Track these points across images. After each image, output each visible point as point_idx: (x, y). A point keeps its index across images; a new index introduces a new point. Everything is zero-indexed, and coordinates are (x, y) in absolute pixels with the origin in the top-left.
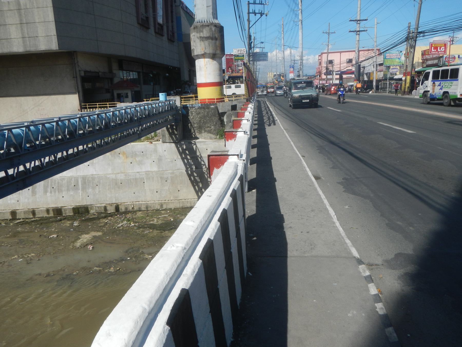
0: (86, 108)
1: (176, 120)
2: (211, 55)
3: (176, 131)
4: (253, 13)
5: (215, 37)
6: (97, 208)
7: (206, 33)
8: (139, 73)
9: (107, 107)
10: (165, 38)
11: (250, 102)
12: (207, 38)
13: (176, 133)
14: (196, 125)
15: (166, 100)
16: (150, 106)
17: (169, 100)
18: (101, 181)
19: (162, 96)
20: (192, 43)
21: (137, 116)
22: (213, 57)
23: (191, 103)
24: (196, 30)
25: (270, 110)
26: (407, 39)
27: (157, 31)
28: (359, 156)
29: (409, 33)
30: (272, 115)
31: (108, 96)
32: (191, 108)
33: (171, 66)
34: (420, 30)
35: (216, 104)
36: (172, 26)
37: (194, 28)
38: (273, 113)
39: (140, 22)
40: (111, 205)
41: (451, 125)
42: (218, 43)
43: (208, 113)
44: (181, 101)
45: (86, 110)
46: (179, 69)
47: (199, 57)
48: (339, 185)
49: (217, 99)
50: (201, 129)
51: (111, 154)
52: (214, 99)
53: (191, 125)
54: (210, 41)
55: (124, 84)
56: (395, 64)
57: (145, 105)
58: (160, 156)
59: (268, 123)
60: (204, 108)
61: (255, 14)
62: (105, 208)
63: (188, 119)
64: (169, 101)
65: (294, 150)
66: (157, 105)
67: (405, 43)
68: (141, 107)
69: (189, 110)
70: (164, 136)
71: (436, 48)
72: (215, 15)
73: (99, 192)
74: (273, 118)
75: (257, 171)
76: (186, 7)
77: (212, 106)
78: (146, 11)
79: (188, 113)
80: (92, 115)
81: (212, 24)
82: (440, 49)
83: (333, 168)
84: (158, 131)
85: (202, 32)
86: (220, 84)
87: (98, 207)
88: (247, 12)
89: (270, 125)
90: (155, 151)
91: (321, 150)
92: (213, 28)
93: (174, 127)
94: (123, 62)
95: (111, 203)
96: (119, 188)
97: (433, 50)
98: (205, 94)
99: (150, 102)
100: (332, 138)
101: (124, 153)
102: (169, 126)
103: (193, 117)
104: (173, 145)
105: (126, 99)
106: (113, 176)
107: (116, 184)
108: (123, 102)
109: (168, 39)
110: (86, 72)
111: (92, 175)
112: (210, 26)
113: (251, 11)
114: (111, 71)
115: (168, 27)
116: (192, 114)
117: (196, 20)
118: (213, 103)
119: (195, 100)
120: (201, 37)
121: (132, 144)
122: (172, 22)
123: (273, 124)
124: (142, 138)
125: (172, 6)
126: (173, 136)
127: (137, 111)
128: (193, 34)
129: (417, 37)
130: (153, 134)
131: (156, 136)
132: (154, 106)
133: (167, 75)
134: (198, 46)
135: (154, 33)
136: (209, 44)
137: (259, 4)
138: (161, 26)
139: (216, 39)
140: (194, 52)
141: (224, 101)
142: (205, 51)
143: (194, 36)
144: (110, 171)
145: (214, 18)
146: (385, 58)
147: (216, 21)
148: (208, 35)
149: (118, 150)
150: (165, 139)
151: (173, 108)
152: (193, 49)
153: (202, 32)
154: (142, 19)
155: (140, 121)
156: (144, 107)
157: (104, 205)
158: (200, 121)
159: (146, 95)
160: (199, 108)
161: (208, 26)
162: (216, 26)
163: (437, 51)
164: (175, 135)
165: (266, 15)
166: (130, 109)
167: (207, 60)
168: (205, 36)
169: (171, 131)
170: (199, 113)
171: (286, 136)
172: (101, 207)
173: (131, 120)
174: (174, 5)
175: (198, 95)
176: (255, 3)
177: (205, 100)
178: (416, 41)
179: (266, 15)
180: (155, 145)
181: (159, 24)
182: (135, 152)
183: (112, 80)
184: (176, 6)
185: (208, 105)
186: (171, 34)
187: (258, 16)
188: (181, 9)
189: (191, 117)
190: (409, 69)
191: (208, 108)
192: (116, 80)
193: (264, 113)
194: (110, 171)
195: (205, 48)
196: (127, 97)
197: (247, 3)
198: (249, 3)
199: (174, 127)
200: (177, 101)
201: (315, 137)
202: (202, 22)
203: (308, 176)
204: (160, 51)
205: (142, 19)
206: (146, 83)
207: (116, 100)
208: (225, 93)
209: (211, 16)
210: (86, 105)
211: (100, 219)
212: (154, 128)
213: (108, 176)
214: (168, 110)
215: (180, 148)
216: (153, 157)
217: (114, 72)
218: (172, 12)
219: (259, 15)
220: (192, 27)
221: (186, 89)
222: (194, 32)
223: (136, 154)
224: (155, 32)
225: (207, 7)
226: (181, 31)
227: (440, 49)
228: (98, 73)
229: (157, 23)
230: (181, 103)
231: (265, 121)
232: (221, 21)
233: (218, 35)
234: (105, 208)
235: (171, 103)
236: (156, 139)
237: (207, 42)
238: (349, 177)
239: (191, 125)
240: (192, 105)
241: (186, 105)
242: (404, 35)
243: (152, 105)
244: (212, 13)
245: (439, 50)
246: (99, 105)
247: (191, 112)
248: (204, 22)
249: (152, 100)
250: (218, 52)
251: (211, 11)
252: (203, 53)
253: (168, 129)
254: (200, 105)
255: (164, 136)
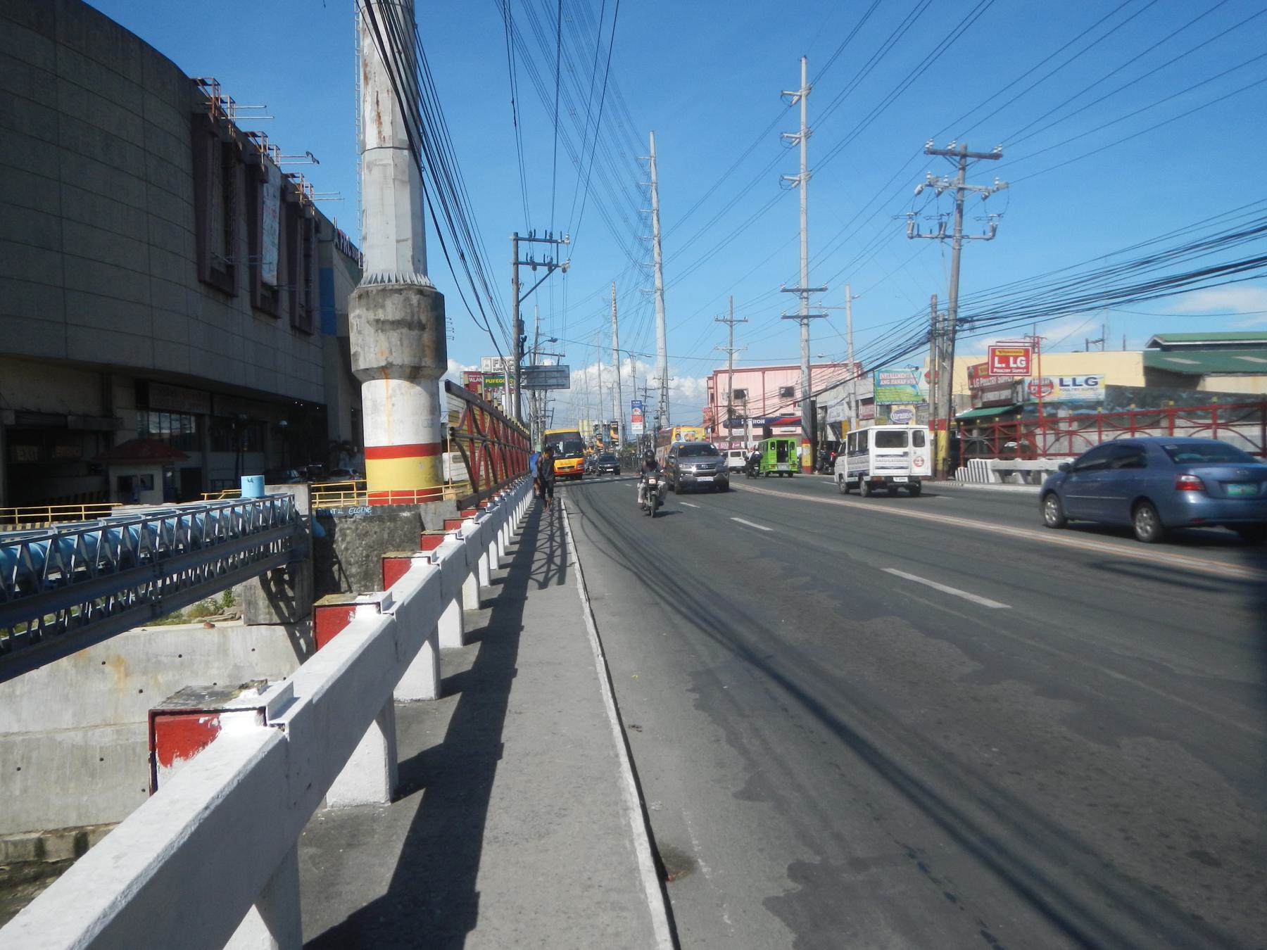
0: (12, 521)
1: (292, 556)
2: (408, 371)
3: (292, 588)
4: (527, 263)
5: (420, 322)
6: (11, 849)
7: (392, 309)
8: (199, 417)
9: (79, 518)
10: (284, 323)
11: (479, 507)
12: (396, 324)
13: (290, 593)
14: (354, 570)
15: (262, 497)
16: (203, 516)
17: (272, 496)
18: (34, 754)
19: (249, 486)
20: (353, 337)
21: (149, 548)
22: (413, 374)
23: (342, 505)
24: (363, 301)
25: (562, 528)
26: (932, 336)
27: (259, 303)
28: (843, 716)
29: (935, 320)
30: (563, 545)
31: (94, 483)
32: (340, 518)
33: (300, 401)
34: (961, 315)
35: (416, 507)
36: (307, 294)
37: (360, 297)
38: (569, 539)
39: (207, 277)
40: (60, 833)
41: (1107, 575)
42: (427, 337)
43: (391, 533)
44: (311, 498)
45: (10, 527)
46: (324, 408)
47: (373, 374)
48: (777, 923)
49: (420, 492)
50: (371, 581)
51: (75, 666)
52: (411, 493)
53: (340, 568)
54: (405, 331)
55: (148, 449)
56: (905, 399)
57: (209, 509)
58: (236, 667)
59: (541, 577)
60: (381, 519)
61: (534, 266)
62: (40, 846)
63: (333, 551)
64: (272, 498)
65: (601, 701)
66: (227, 512)
67: (928, 346)
68: (131, 528)
69: (335, 525)
70: (251, 603)
71: (1005, 360)
72: (420, 263)
73: (25, 790)
74: (565, 554)
75: (408, 843)
76: (351, 246)
77: (406, 514)
78: (228, 250)
79: (331, 534)
80: (34, 541)
81: (411, 286)
82: (1015, 362)
83: (749, 798)
84: (237, 589)
85: (383, 307)
86: (433, 450)
87: (15, 844)
88: (512, 259)
89: (543, 585)
90: (223, 650)
91: (705, 688)
92: (415, 299)
93: (286, 577)
94: (148, 388)
95: (61, 826)
96: (93, 775)
97: (997, 365)
98: (385, 477)
99: (204, 503)
100: (749, 636)
101: (119, 661)
102: (269, 574)
103: (347, 545)
104: (281, 631)
105: (148, 492)
106: (77, 737)
107: (85, 762)
108: (136, 501)
109: (293, 327)
110: (20, 413)
111: (6, 735)
112: (404, 293)
113: (522, 258)
114: (107, 412)
115: (292, 295)
116: (344, 535)
117: (366, 275)
118: (409, 505)
119: (359, 495)
120: (378, 321)
121: (136, 631)
122: (307, 281)
123: (555, 579)
124: (186, 610)
125: (307, 240)
126: (282, 604)
127: (154, 532)
128: (357, 312)
129: (955, 332)
130: (219, 597)
131: (229, 602)
132: (216, 514)
133: (285, 423)
134: (369, 344)
135: (248, 310)
136: (401, 340)
137: (545, 241)
138: (273, 292)
139: (422, 327)
140: (357, 360)
141: (440, 498)
142: (390, 360)
143: (359, 316)
144: (67, 719)
145: (416, 271)
146: (877, 384)
147: (423, 281)
148: (398, 316)
149: (92, 651)
150: (256, 615)
151: (283, 521)
152: (355, 354)
153: (383, 307)
154: (213, 270)
155: (161, 562)
156: (180, 521)
157: (35, 836)
158: (367, 556)
159: (213, 481)
160: (367, 518)
161: (399, 291)
162: (420, 291)
163: (1008, 367)
164: (288, 601)
165: (564, 271)
166: (126, 527)
167: (394, 383)
168: (390, 318)
169: (273, 589)
170: (366, 534)
171: (585, 633)
172: (24, 843)
173: (129, 559)
174: (313, 239)
175: (368, 480)
176: (532, 238)
177: (385, 494)
178: (953, 341)
179: (564, 271)
180: (224, 630)
181: (266, 286)
182: (156, 656)
183: (108, 436)
184: (320, 241)
185: (393, 511)
186: (303, 314)
187: (543, 271)
188: (334, 250)
189: (340, 546)
190: (943, 413)
191: (393, 518)
192: (122, 438)
193: (542, 538)
194: (67, 719)
195: (391, 352)
196: (152, 488)
197: (512, 237)
198: (517, 239)
199: (286, 577)
200: (298, 497)
201: (689, 630)
202: (382, 281)
203: (634, 870)
204: (258, 356)
205: (213, 270)
206: (218, 446)
207: (113, 495)
208: (447, 477)
209: (410, 267)
210: (13, 512)
211: (16, 885)
212: (226, 580)
213: (59, 737)
214: (265, 528)
215: (302, 641)
216: (214, 671)
217: (119, 413)
218: (307, 256)
219: (545, 270)
220: (355, 294)
221: (341, 464)
222: (360, 306)
223: (159, 662)
224: (254, 307)
225: (398, 241)
226: (333, 306)
227: (1015, 362)
228: (65, 417)
229: (259, 285)
230: (311, 503)
231: (534, 567)
232: (439, 278)
233: (427, 321)
234: (40, 846)
235: (278, 503)
236: (228, 612)
237: (394, 336)
238: (817, 860)
239: (340, 568)
240: (346, 509)
241: (327, 510)
242: (921, 327)
243: (208, 511)
244: (413, 257)
245: (1012, 365)
246: (53, 510)
247: (341, 530)
248: (390, 280)
249: (227, 497)
250: (427, 363)
251: (408, 252)
252: (383, 364)
253: (265, 584)
254: (368, 510)
255: (251, 603)
